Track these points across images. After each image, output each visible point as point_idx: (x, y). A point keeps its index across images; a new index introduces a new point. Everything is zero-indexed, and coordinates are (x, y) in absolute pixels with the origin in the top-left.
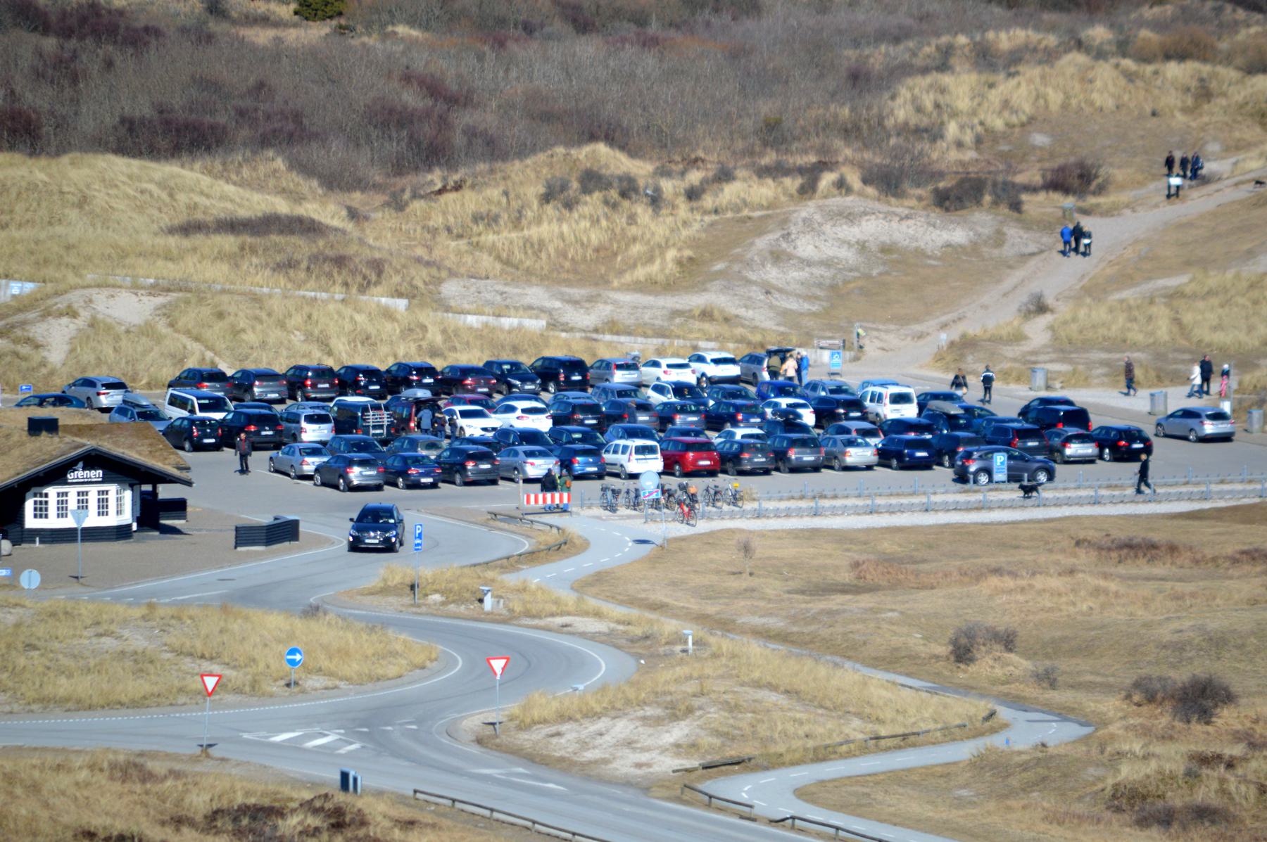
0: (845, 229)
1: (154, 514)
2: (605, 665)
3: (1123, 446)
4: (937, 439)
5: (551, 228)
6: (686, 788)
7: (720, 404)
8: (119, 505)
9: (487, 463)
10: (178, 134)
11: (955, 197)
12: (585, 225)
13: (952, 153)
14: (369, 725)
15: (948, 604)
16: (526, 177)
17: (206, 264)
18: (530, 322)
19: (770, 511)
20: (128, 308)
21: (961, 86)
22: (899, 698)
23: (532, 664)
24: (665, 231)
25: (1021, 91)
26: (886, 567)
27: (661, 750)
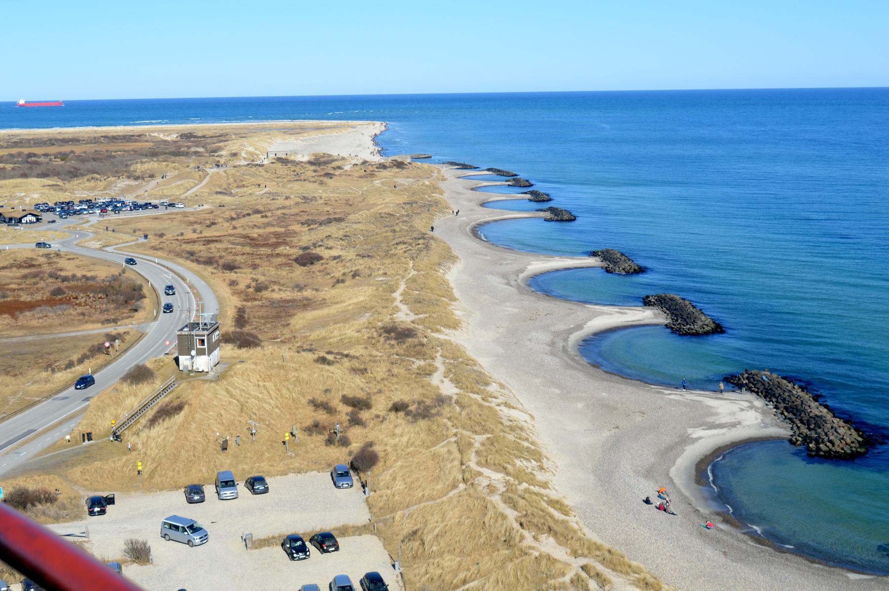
0: (123, 183)
1: (38, 220)
2: (91, 235)
3: (155, 207)
4: (136, 206)
5: (88, 184)
6: (100, 249)
7: (108, 204)
8: (34, 219)
9: (80, 212)
10: (44, 175)
11: (137, 178)
12: (92, 184)
13: (138, 174)
14: (63, 244)
15: (133, 226)
16: (85, 178)
17: (46, 190)
18: (85, 195)
19: (112, 217)
20: (36, 196)
21: (139, 166)
22: (126, 237)
23: (82, 236)
24: (102, 184)
25: (146, 166)
26: (126, 222)
27: (97, 245)
